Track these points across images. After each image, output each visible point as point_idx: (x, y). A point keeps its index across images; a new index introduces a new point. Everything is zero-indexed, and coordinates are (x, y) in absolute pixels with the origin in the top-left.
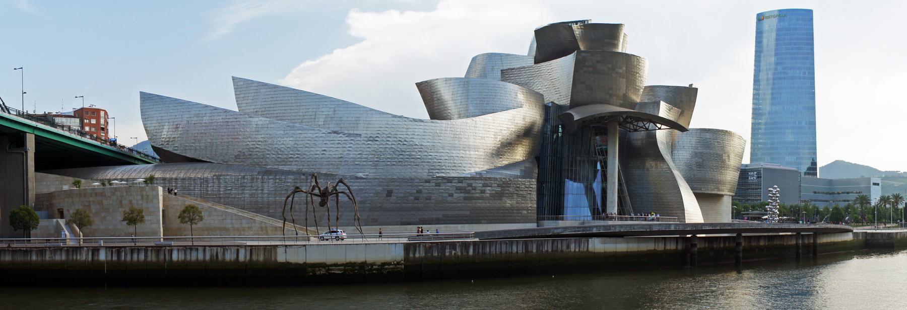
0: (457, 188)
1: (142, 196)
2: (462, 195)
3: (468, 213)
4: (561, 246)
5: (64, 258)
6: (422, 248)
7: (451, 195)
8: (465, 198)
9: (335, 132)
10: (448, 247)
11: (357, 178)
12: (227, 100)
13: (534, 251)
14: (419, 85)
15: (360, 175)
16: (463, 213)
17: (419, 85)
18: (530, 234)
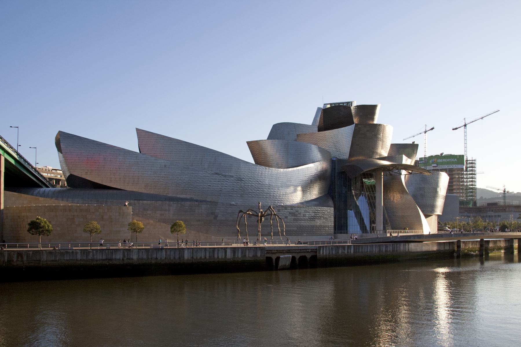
0: (290, 213)
1: (120, 213)
2: (293, 217)
3: (295, 229)
4: (402, 247)
5: (104, 257)
6: (327, 248)
7: (286, 217)
8: (294, 220)
9: (216, 174)
10: (340, 248)
11: (231, 205)
12: (132, 145)
13: (384, 250)
14: (249, 143)
15: (233, 203)
16: (292, 229)
17: (249, 143)
18: (377, 241)
